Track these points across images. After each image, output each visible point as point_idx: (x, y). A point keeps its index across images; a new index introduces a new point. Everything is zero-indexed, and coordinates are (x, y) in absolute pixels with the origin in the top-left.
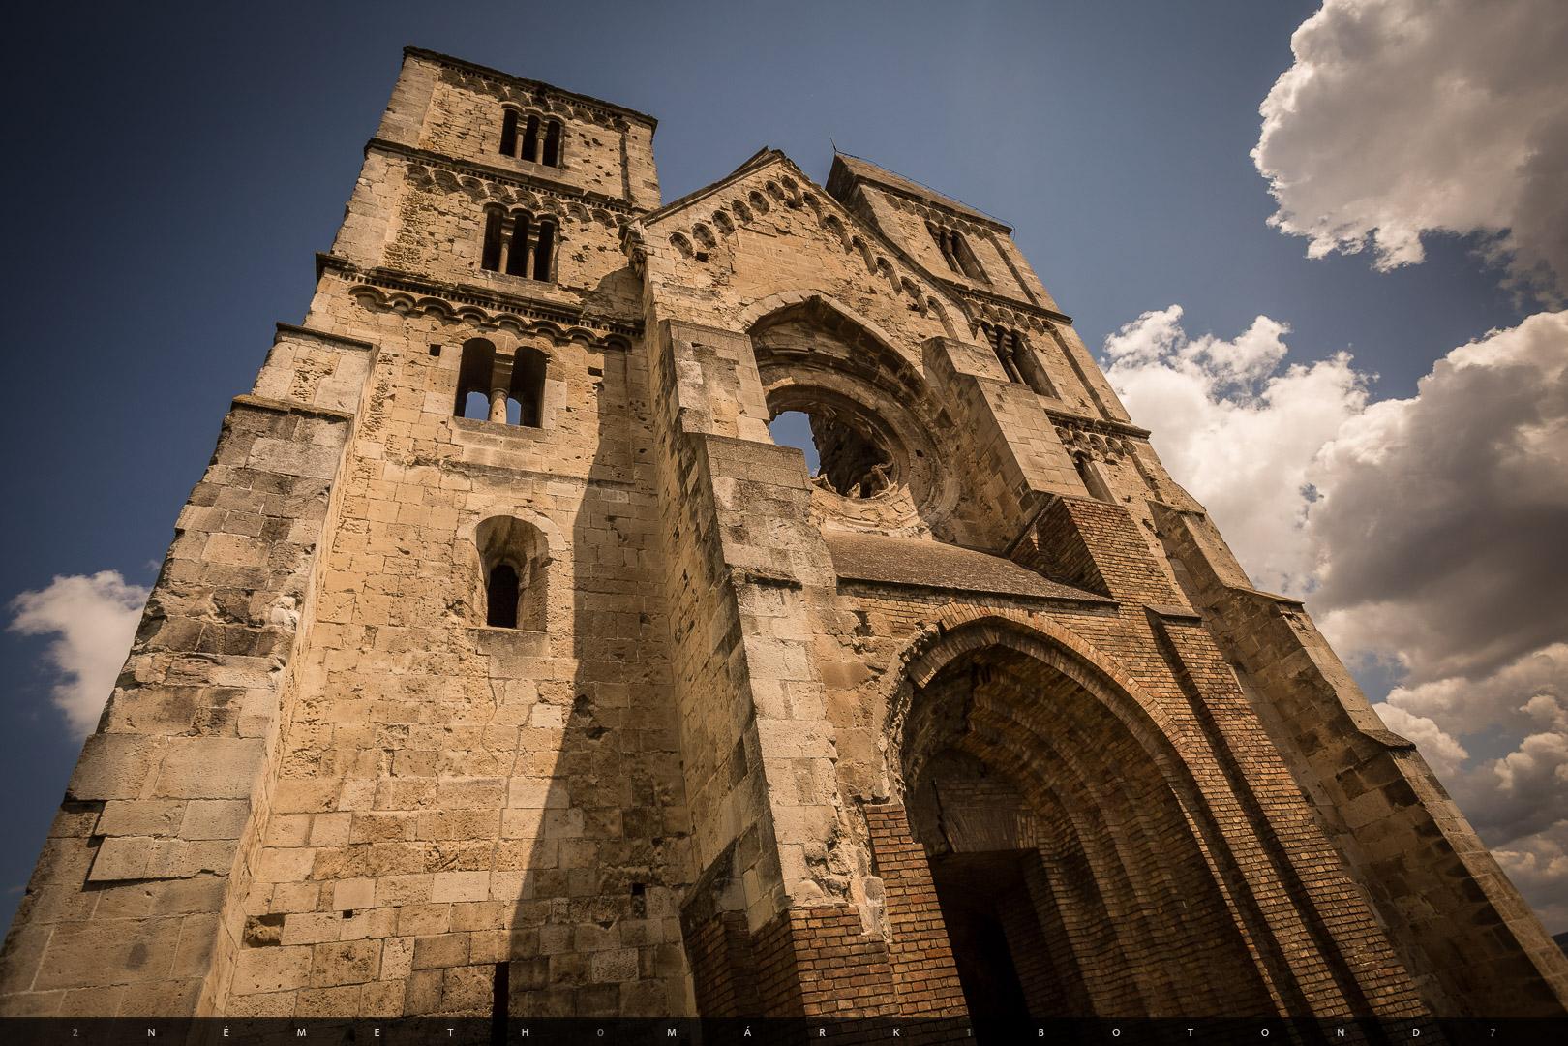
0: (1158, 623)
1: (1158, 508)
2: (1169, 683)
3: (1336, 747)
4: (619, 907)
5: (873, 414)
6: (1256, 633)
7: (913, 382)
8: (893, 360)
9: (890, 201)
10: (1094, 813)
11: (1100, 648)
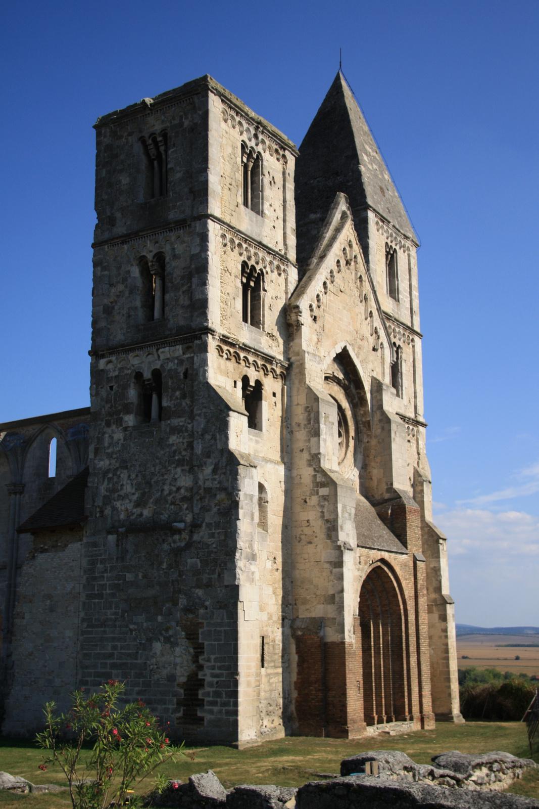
0: (415, 560)
1: (417, 474)
2: (412, 584)
3: (434, 596)
6: (428, 545)
7: (363, 400)
8: (359, 384)
9: (377, 223)
11: (401, 570)
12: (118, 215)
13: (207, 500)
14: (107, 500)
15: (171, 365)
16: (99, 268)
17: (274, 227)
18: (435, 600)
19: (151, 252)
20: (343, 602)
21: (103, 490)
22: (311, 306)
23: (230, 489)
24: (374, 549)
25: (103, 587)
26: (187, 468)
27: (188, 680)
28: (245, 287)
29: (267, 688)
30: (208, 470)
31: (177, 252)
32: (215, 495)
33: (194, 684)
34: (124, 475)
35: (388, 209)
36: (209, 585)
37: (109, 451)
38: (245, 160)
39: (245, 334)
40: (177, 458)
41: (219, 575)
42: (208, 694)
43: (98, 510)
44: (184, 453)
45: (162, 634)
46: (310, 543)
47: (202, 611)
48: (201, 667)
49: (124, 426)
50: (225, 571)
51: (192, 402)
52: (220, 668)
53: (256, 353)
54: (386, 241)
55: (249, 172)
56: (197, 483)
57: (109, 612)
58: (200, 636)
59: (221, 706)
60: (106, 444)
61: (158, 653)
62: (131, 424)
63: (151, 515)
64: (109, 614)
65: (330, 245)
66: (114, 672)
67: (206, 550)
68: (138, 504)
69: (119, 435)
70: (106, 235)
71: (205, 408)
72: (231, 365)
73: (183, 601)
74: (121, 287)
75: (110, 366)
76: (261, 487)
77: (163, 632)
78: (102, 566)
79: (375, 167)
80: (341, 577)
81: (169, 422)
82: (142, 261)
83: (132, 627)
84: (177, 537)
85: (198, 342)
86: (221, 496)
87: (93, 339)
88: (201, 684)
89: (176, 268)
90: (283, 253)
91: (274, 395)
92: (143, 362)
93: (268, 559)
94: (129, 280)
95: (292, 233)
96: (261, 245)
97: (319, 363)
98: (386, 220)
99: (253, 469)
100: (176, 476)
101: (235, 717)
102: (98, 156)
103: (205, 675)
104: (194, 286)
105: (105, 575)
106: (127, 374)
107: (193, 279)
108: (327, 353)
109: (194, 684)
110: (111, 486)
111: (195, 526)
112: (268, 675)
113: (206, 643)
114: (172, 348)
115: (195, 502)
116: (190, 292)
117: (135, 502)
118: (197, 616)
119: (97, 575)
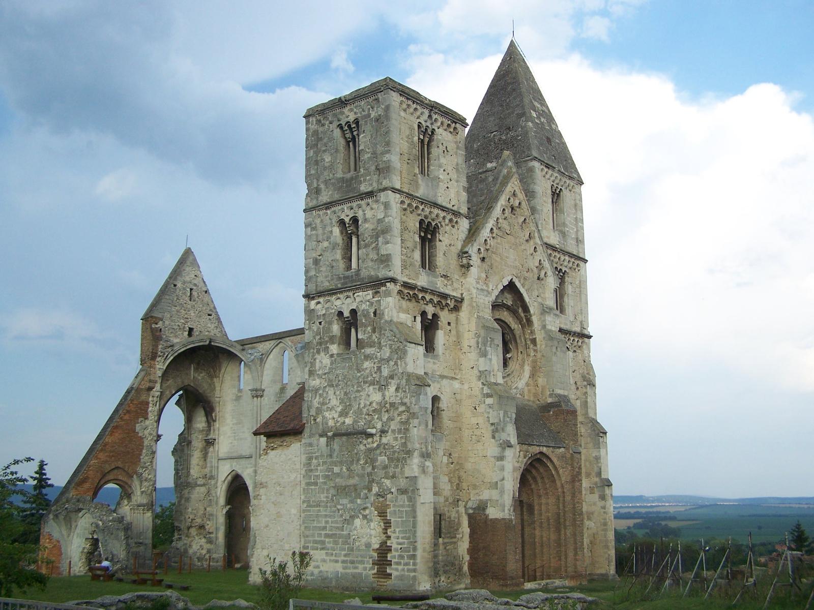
4: (455, 504)
5: (512, 331)
7: (529, 322)
8: (526, 309)
10: (540, 496)
12: (322, 186)
13: (392, 413)
14: (319, 411)
15: (364, 306)
16: (309, 229)
17: (448, 188)
18: (596, 484)
19: (348, 216)
20: (503, 488)
21: (316, 403)
22: (479, 249)
23: (408, 404)
24: (534, 445)
25: (317, 476)
26: (377, 387)
27: (380, 547)
28: (423, 240)
29: (444, 553)
30: (392, 389)
31: (367, 216)
32: (397, 408)
33: (384, 550)
34: (331, 391)
35: (553, 156)
36: (393, 477)
37: (320, 372)
38: (422, 137)
39: (422, 280)
40: (369, 379)
41: (401, 469)
42: (394, 557)
43: (312, 418)
44: (374, 375)
45: (360, 513)
46: (479, 441)
47: (389, 496)
48: (389, 537)
49: (330, 353)
50: (405, 466)
51: (380, 335)
52: (402, 538)
53: (433, 292)
54: (552, 183)
55: (426, 146)
56: (384, 399)
57: (322, 495)
58: (388, 514)
59: (404, 565)
60: (317, 368)
61: (358, 527)
62: (335, 352)
63: (351, 423)
64: (322, 497)
65: (496, 199)
66: (327, 540)
67: (392, 450)
68: (344, 414)
69: (327, 361)
70: (314, 203)
71: (390, 340)
72: (412, 305)
73: (375, 489)
74: (326, 244)
75: (319, 306)
76: (435, 399)
77: (361, 511)
78: (316, 461)
79: (542, 120)
80: (502, 469)
81: (363, 351)
82: (342, 222)
83: (339, 507)
84: (370, 440)
85: (383, 288)
86: (402, 409)
87: (306, 286)
88: (389, 549)
89: (366, 228)
90: (455, 208)
91: (449, 324)
92: (345, 303)
93: (444, 455)
94: (332, 239)
95: (464, 191)
96: (435, 205)
97: (487, 296)
98: (551, 166)
99: (428, 388)
100: (369, 393)
101: (413, 574)
102: (307, 139)
103: (392, 543)
104: (380, 244)
105: (319, 468)
106: (331, 313)
107: (379, 239)
108: (495, 287)
109: (384, 550)
110: (322, 399)
111: (383, 432)
112: (444, 544)
113: (393, 520)
114: (366, 293)
115: (383, 413)
116: (377, 248)
117: (340, 412)
118: (386, 499)
119: (312, 467)
